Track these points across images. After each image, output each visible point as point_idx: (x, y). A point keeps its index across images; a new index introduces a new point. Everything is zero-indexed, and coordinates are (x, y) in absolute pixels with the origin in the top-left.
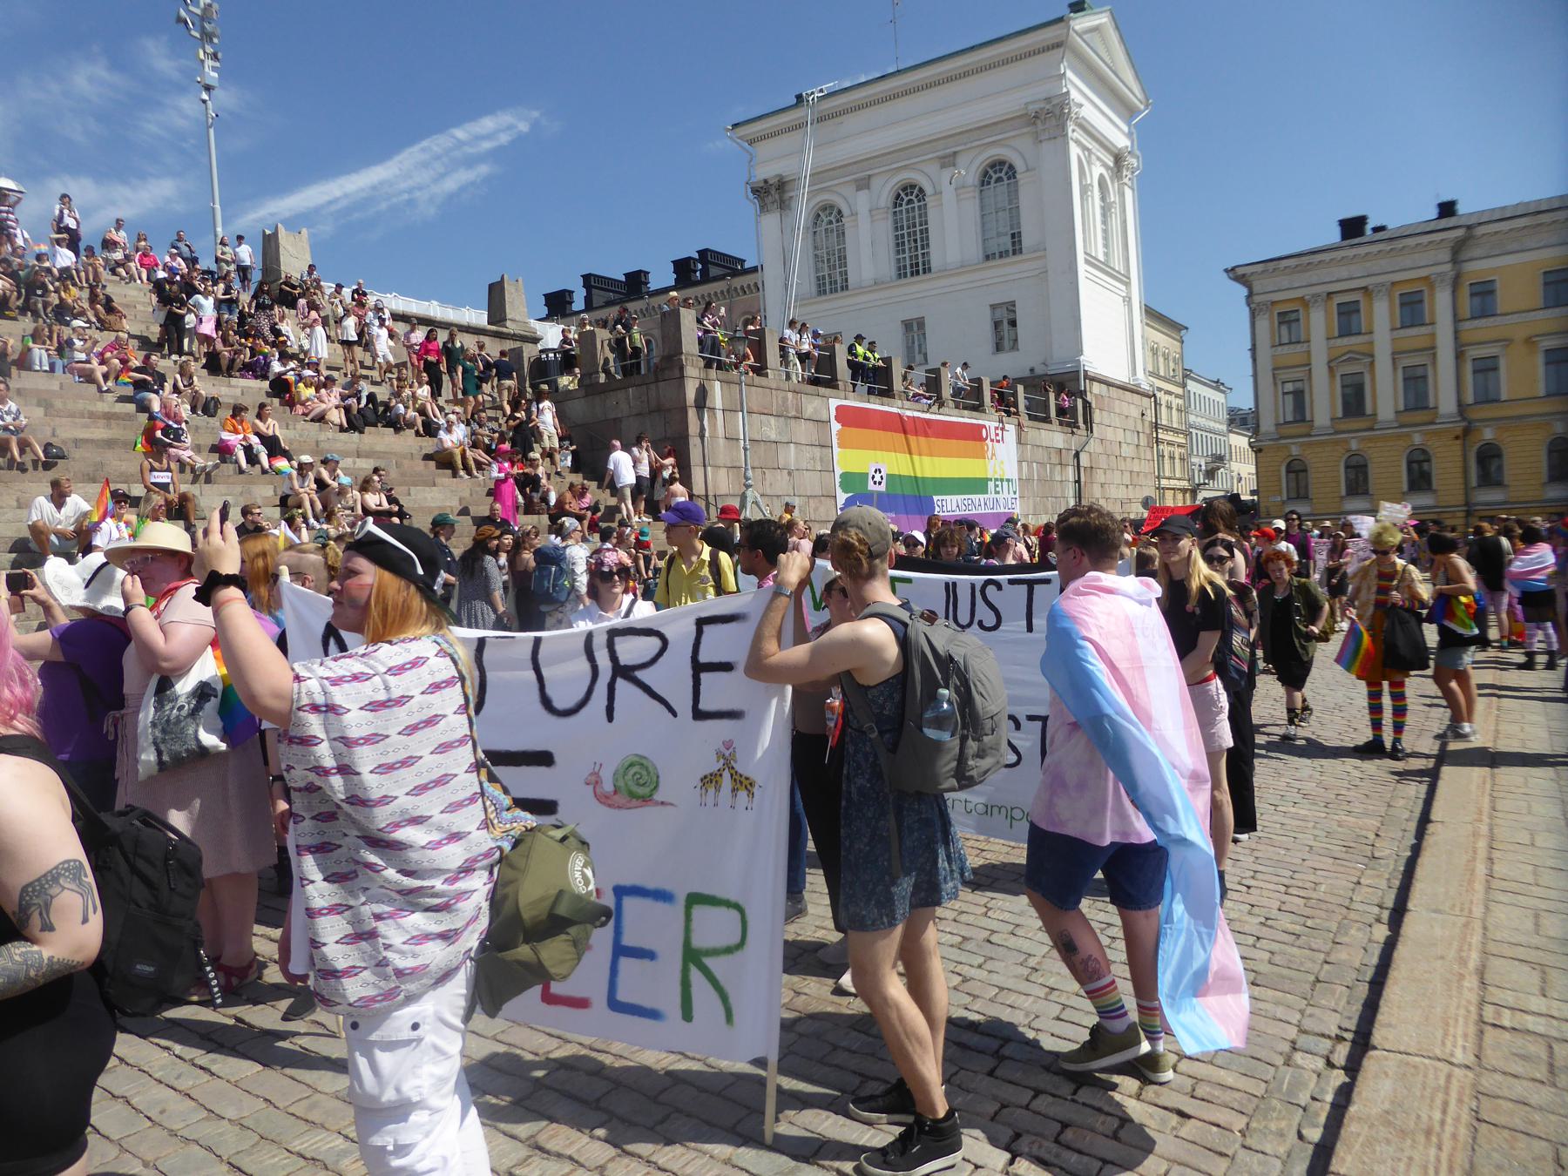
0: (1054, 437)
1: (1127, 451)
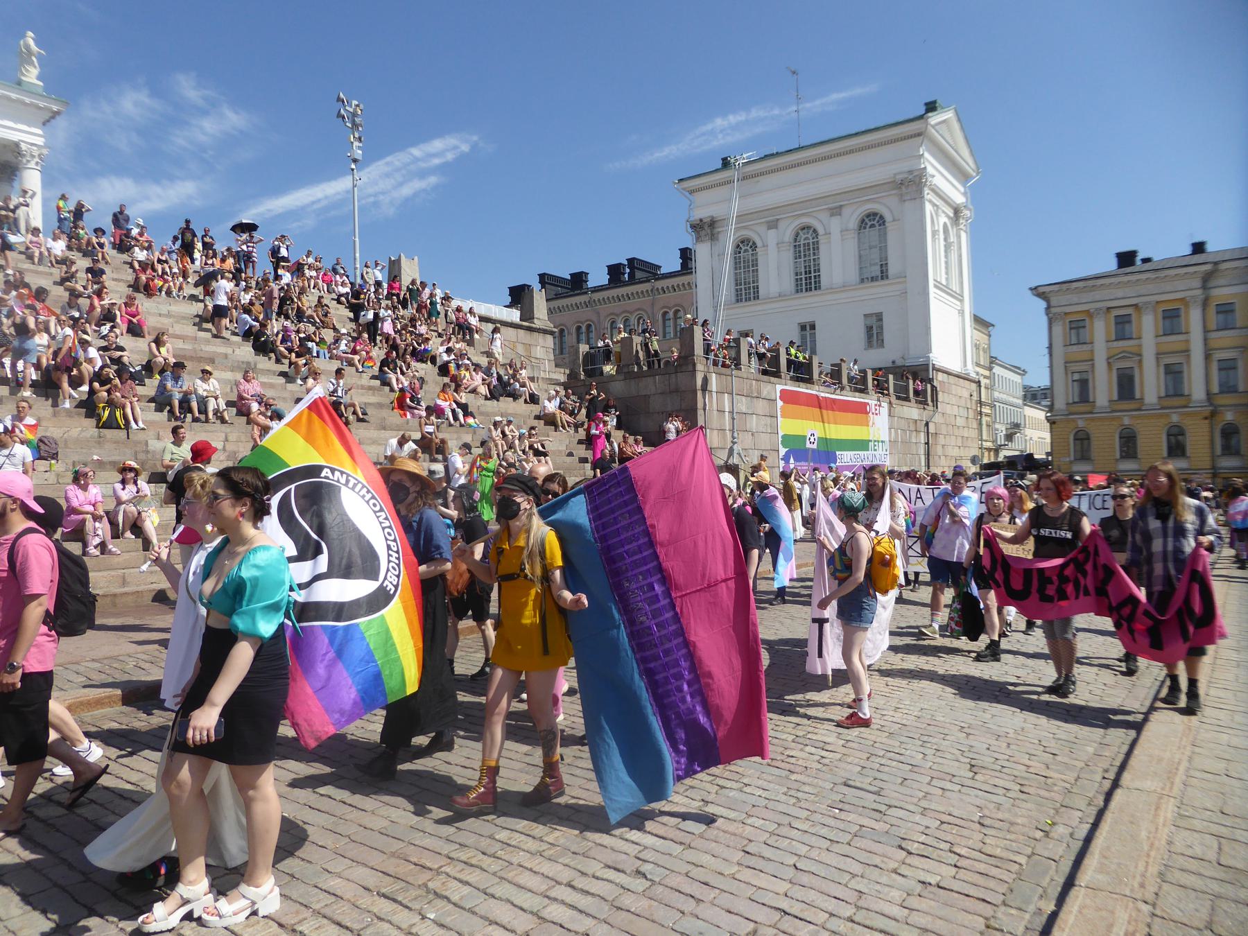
0: (912, 411)
1: (960, 422)
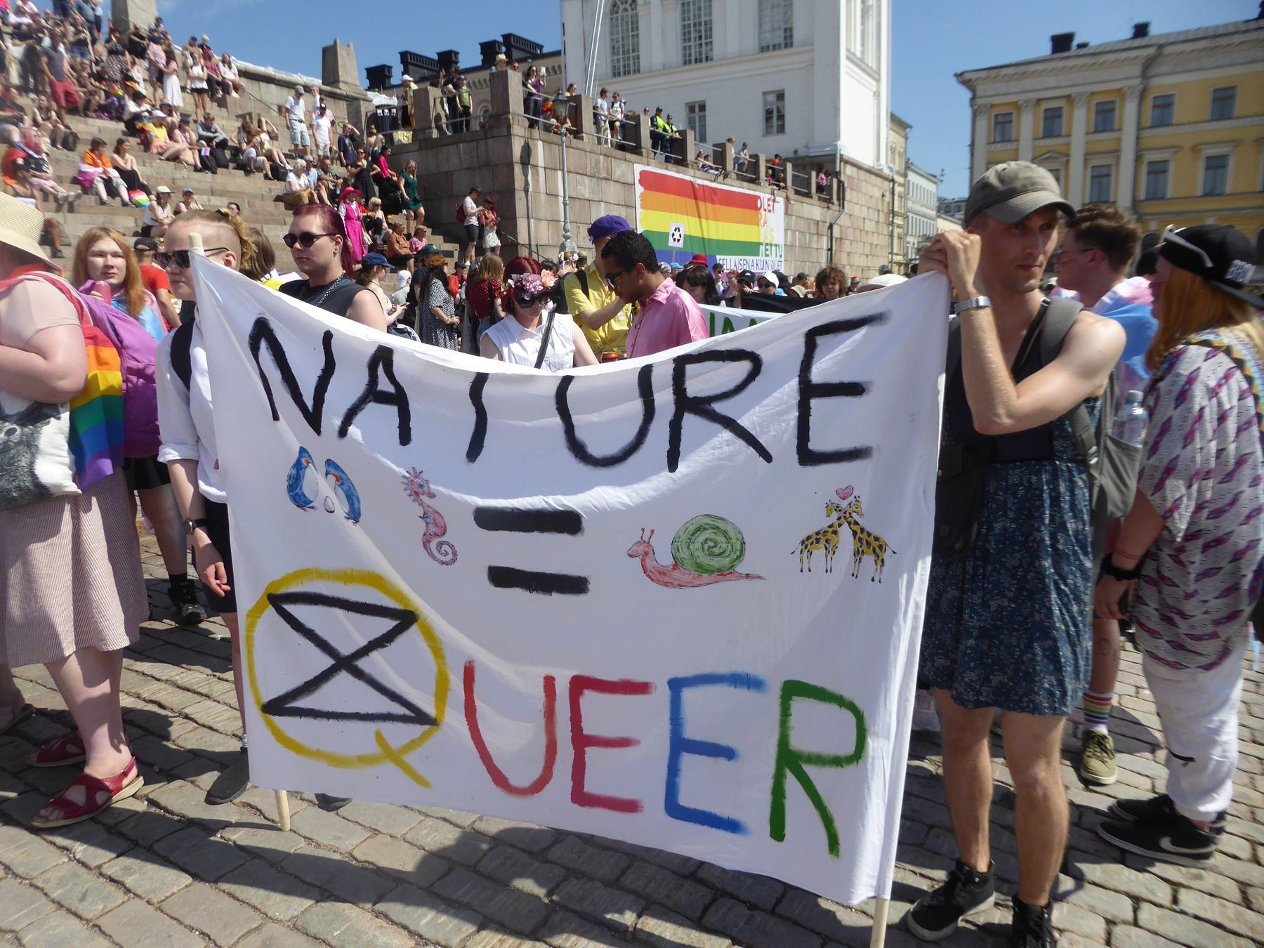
0: (813, 210)
1: (869, 226)
